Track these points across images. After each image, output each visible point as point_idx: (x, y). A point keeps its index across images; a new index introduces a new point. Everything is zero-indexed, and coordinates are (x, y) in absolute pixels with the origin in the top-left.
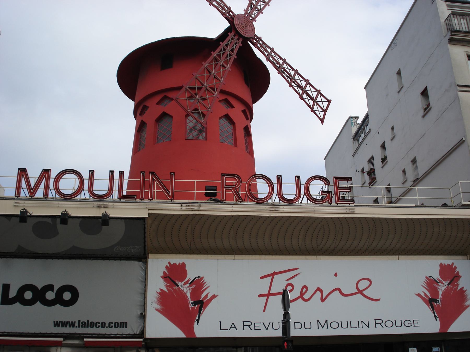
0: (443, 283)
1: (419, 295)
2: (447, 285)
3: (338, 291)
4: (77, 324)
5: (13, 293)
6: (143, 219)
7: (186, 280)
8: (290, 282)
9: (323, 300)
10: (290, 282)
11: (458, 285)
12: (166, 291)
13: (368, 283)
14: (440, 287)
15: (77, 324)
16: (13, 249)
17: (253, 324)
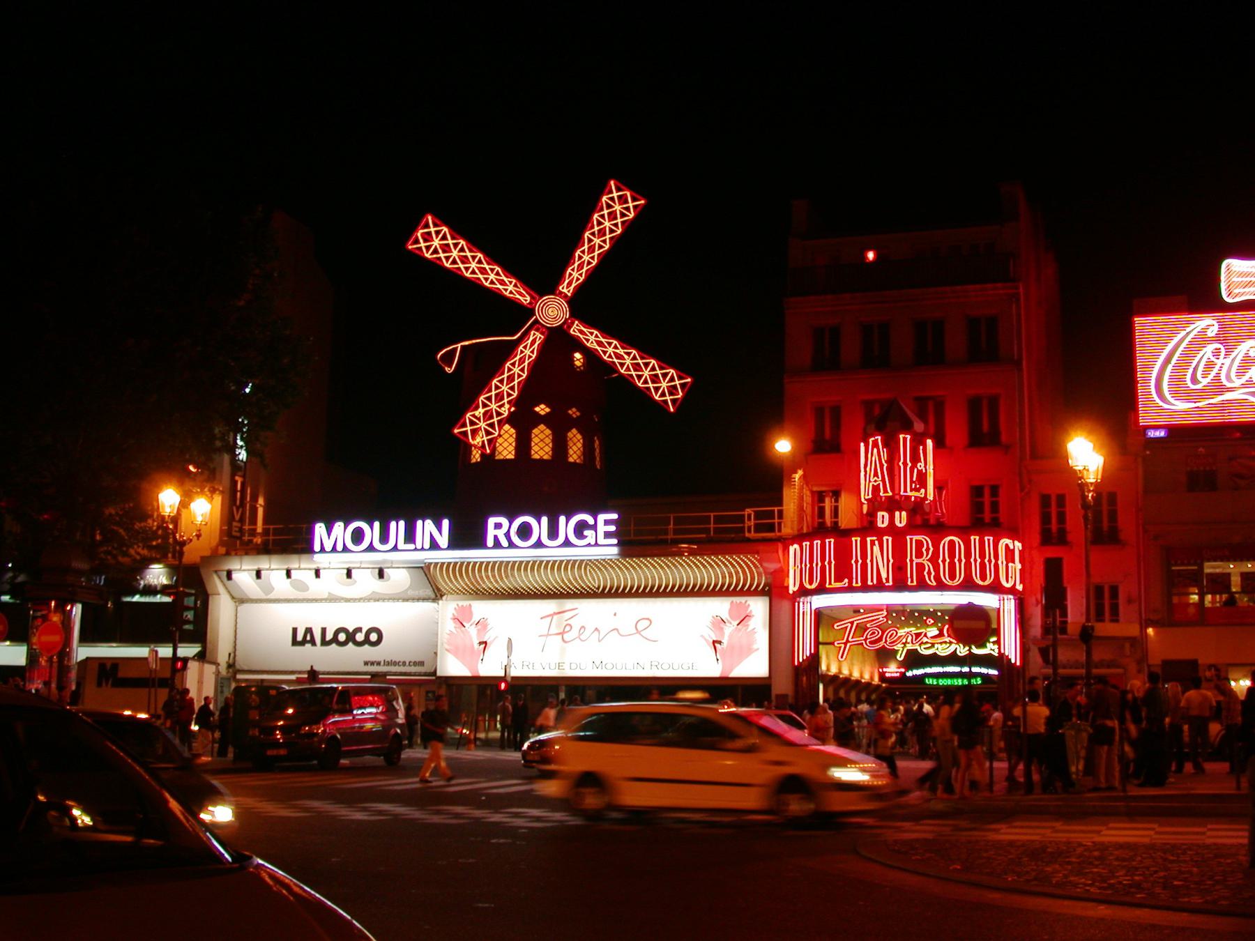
0: (731, 623)
1: (702, 636)
2: (736, 626)
3: (616, 631)
4: (382, 663)
5: (329, 636)
6: (422, 568)
7: (472, 621)
8: (569, 622)
9: (599, 641)
10: (569, 622)
11: (748, 625)
12: (455, 631)
13: (648, 622)
14: (725, 627)
15: (382, 663)
16: (326, 597)
17: (531, 665)
